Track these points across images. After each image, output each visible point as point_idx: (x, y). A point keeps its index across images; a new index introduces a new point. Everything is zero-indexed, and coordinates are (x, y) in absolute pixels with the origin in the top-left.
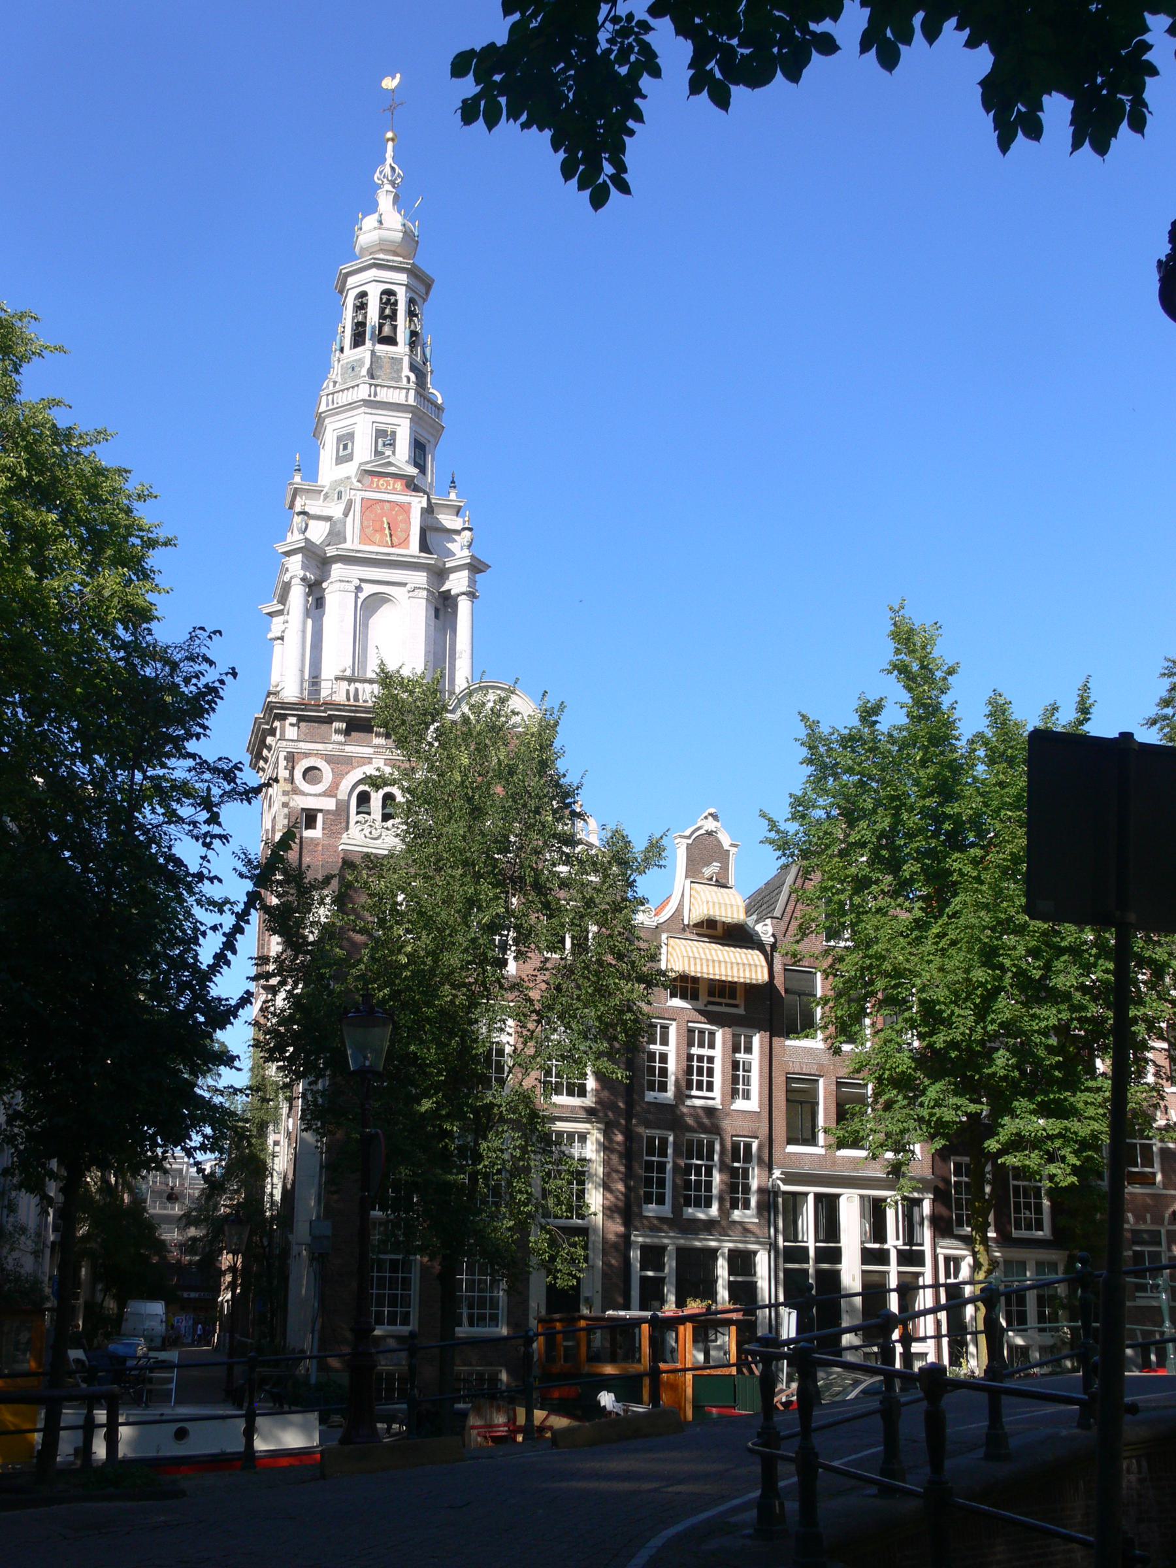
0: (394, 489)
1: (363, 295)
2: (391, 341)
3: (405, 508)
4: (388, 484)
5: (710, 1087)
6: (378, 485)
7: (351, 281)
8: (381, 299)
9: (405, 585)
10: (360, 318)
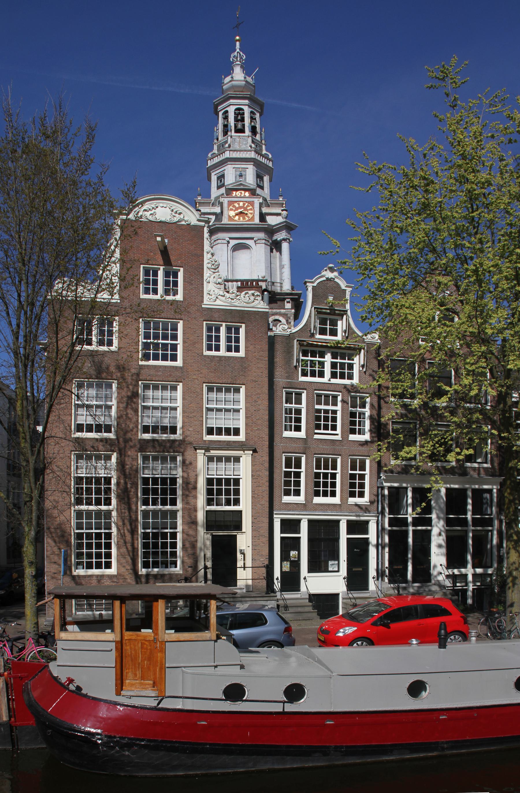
0: (245, 195)
1: (227, 112)
2: (242, 131)
3: (252, 204)
4: (241, 193)
5: (334, 428)
8: (235, 113)
10: (226, 123)
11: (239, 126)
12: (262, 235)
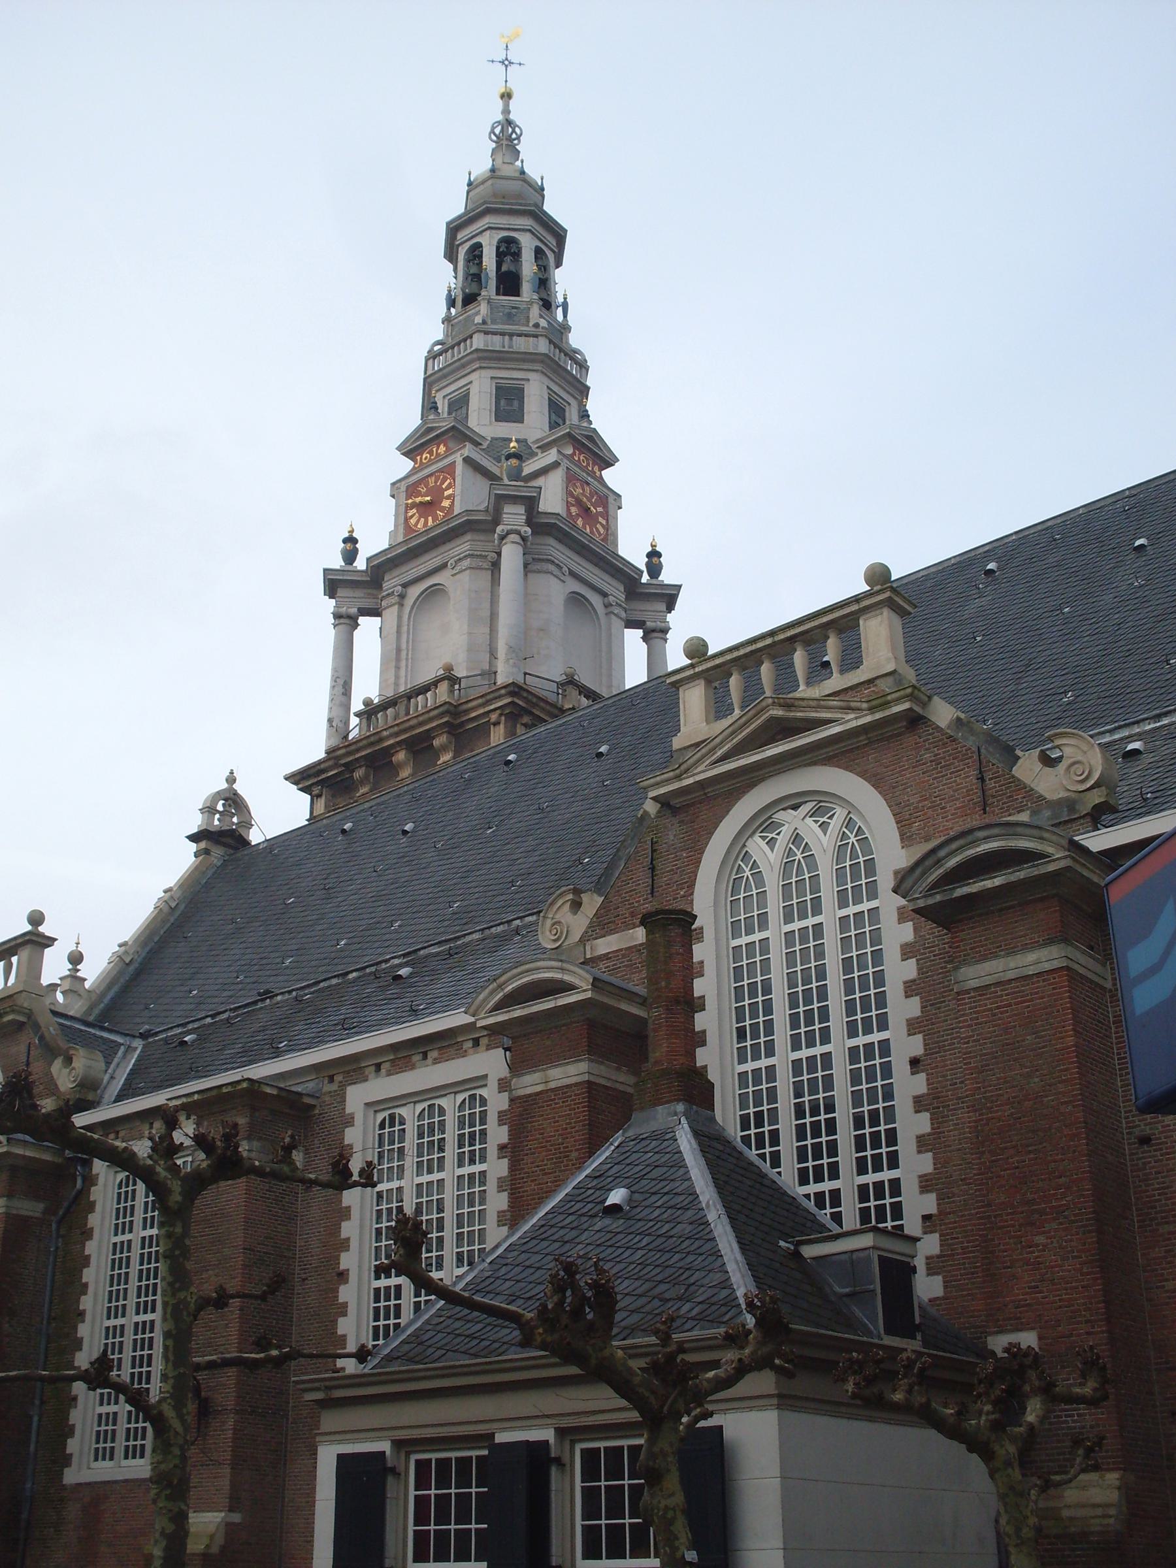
1: (479, 246)
7: (461, 236)
8: (498, 248)
10: (474, 270)
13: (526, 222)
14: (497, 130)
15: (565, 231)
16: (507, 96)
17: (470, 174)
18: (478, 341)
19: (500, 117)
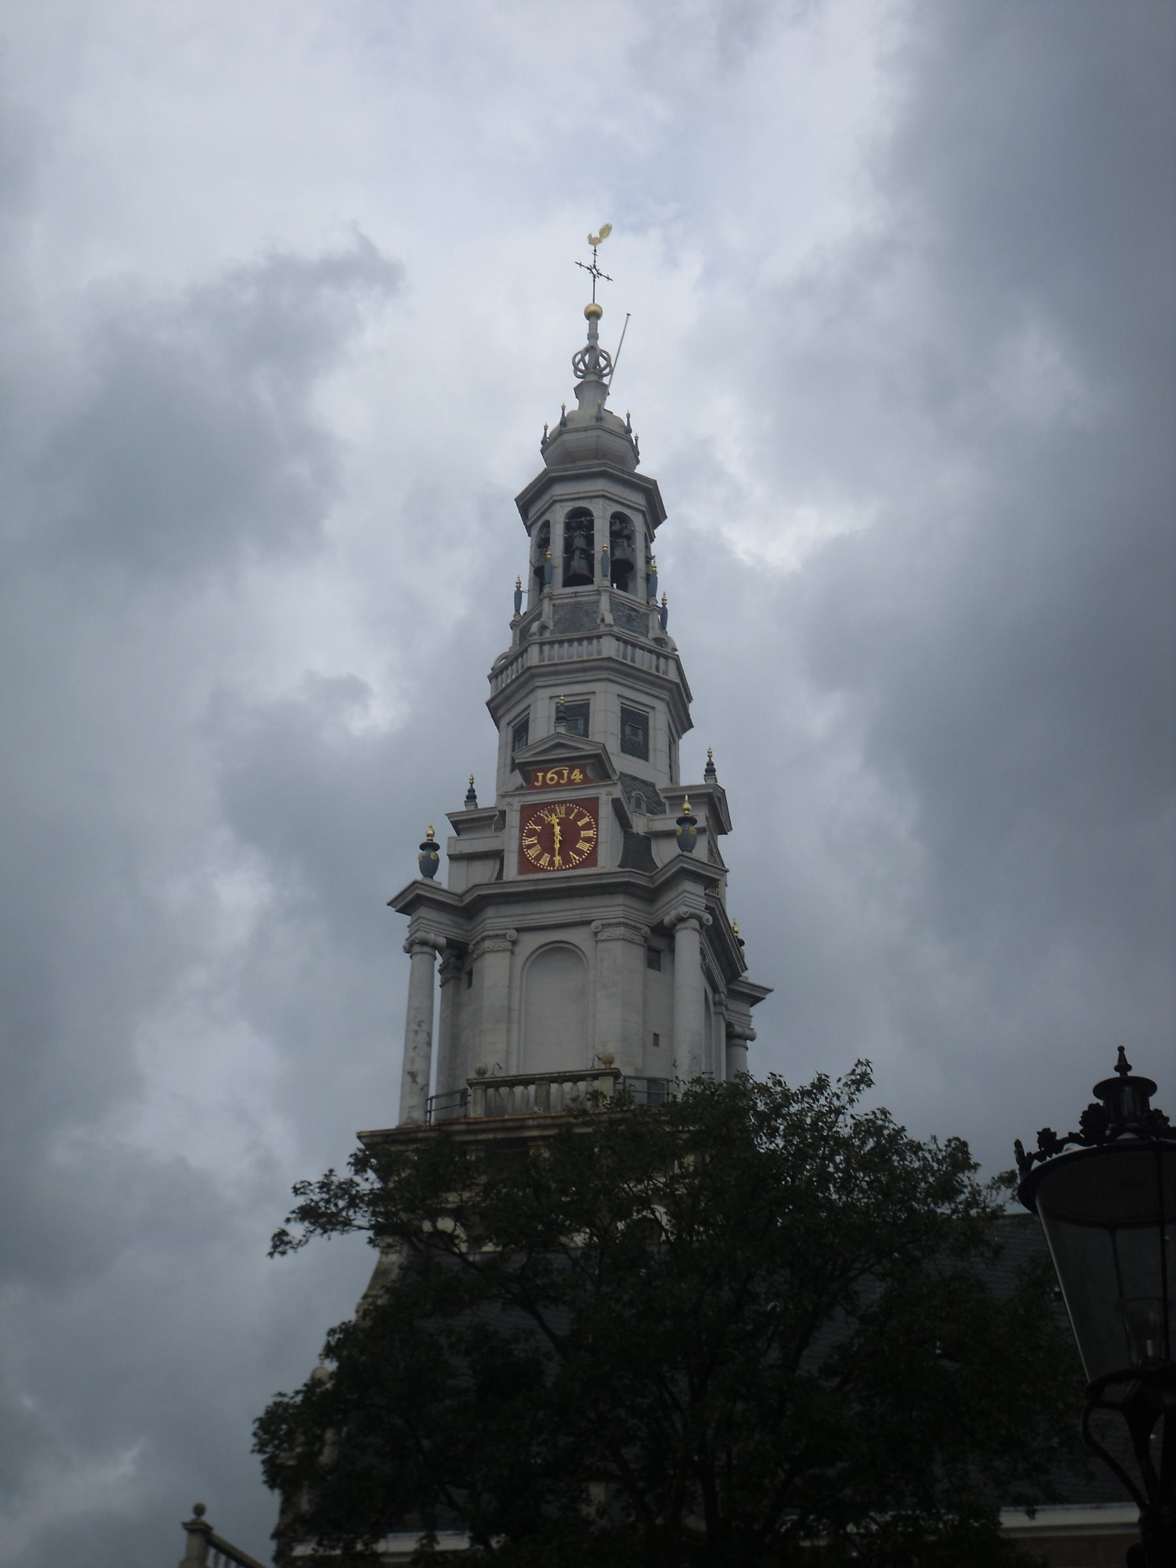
0: (571, 782)
1: (547, 525)
3: (591, 806)
4: (560, 774)
6: (544, 777)
7: (533, 511)
9: (589, 923)
11: (578, 564)
12: (615, 908)
13: (600, 485)
14: (581, 366)
15: (654, 483)
16: (593, 315)
17: (546, 428)
18: (533, 657)
19: (584, 343)
